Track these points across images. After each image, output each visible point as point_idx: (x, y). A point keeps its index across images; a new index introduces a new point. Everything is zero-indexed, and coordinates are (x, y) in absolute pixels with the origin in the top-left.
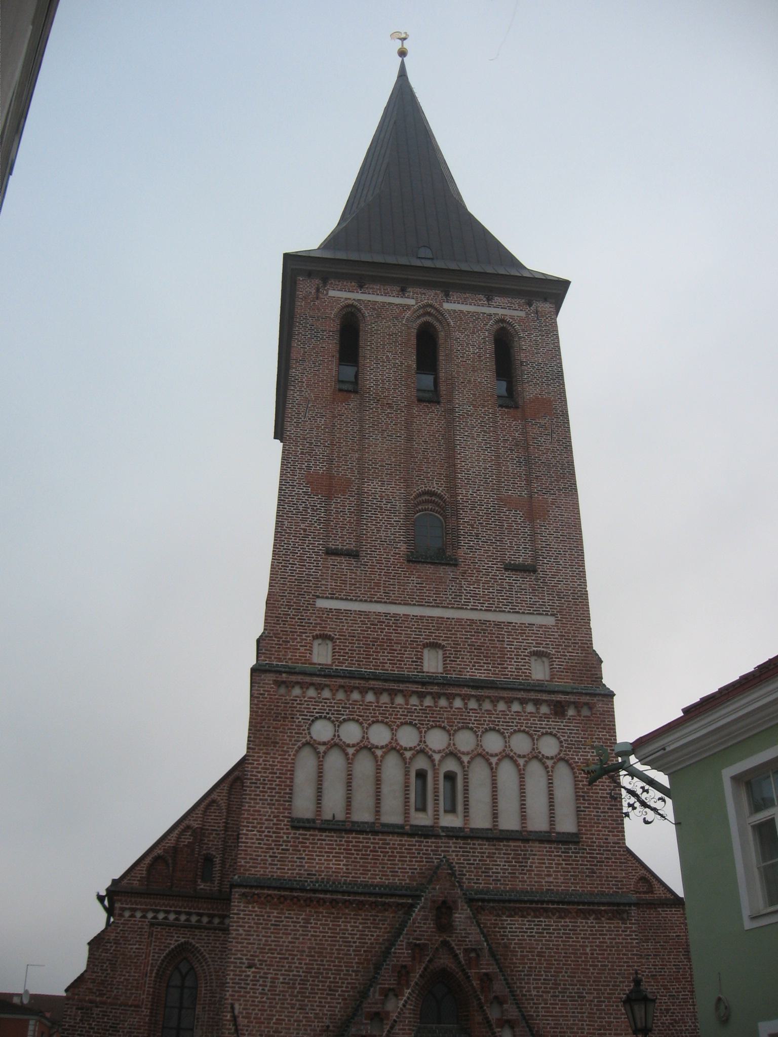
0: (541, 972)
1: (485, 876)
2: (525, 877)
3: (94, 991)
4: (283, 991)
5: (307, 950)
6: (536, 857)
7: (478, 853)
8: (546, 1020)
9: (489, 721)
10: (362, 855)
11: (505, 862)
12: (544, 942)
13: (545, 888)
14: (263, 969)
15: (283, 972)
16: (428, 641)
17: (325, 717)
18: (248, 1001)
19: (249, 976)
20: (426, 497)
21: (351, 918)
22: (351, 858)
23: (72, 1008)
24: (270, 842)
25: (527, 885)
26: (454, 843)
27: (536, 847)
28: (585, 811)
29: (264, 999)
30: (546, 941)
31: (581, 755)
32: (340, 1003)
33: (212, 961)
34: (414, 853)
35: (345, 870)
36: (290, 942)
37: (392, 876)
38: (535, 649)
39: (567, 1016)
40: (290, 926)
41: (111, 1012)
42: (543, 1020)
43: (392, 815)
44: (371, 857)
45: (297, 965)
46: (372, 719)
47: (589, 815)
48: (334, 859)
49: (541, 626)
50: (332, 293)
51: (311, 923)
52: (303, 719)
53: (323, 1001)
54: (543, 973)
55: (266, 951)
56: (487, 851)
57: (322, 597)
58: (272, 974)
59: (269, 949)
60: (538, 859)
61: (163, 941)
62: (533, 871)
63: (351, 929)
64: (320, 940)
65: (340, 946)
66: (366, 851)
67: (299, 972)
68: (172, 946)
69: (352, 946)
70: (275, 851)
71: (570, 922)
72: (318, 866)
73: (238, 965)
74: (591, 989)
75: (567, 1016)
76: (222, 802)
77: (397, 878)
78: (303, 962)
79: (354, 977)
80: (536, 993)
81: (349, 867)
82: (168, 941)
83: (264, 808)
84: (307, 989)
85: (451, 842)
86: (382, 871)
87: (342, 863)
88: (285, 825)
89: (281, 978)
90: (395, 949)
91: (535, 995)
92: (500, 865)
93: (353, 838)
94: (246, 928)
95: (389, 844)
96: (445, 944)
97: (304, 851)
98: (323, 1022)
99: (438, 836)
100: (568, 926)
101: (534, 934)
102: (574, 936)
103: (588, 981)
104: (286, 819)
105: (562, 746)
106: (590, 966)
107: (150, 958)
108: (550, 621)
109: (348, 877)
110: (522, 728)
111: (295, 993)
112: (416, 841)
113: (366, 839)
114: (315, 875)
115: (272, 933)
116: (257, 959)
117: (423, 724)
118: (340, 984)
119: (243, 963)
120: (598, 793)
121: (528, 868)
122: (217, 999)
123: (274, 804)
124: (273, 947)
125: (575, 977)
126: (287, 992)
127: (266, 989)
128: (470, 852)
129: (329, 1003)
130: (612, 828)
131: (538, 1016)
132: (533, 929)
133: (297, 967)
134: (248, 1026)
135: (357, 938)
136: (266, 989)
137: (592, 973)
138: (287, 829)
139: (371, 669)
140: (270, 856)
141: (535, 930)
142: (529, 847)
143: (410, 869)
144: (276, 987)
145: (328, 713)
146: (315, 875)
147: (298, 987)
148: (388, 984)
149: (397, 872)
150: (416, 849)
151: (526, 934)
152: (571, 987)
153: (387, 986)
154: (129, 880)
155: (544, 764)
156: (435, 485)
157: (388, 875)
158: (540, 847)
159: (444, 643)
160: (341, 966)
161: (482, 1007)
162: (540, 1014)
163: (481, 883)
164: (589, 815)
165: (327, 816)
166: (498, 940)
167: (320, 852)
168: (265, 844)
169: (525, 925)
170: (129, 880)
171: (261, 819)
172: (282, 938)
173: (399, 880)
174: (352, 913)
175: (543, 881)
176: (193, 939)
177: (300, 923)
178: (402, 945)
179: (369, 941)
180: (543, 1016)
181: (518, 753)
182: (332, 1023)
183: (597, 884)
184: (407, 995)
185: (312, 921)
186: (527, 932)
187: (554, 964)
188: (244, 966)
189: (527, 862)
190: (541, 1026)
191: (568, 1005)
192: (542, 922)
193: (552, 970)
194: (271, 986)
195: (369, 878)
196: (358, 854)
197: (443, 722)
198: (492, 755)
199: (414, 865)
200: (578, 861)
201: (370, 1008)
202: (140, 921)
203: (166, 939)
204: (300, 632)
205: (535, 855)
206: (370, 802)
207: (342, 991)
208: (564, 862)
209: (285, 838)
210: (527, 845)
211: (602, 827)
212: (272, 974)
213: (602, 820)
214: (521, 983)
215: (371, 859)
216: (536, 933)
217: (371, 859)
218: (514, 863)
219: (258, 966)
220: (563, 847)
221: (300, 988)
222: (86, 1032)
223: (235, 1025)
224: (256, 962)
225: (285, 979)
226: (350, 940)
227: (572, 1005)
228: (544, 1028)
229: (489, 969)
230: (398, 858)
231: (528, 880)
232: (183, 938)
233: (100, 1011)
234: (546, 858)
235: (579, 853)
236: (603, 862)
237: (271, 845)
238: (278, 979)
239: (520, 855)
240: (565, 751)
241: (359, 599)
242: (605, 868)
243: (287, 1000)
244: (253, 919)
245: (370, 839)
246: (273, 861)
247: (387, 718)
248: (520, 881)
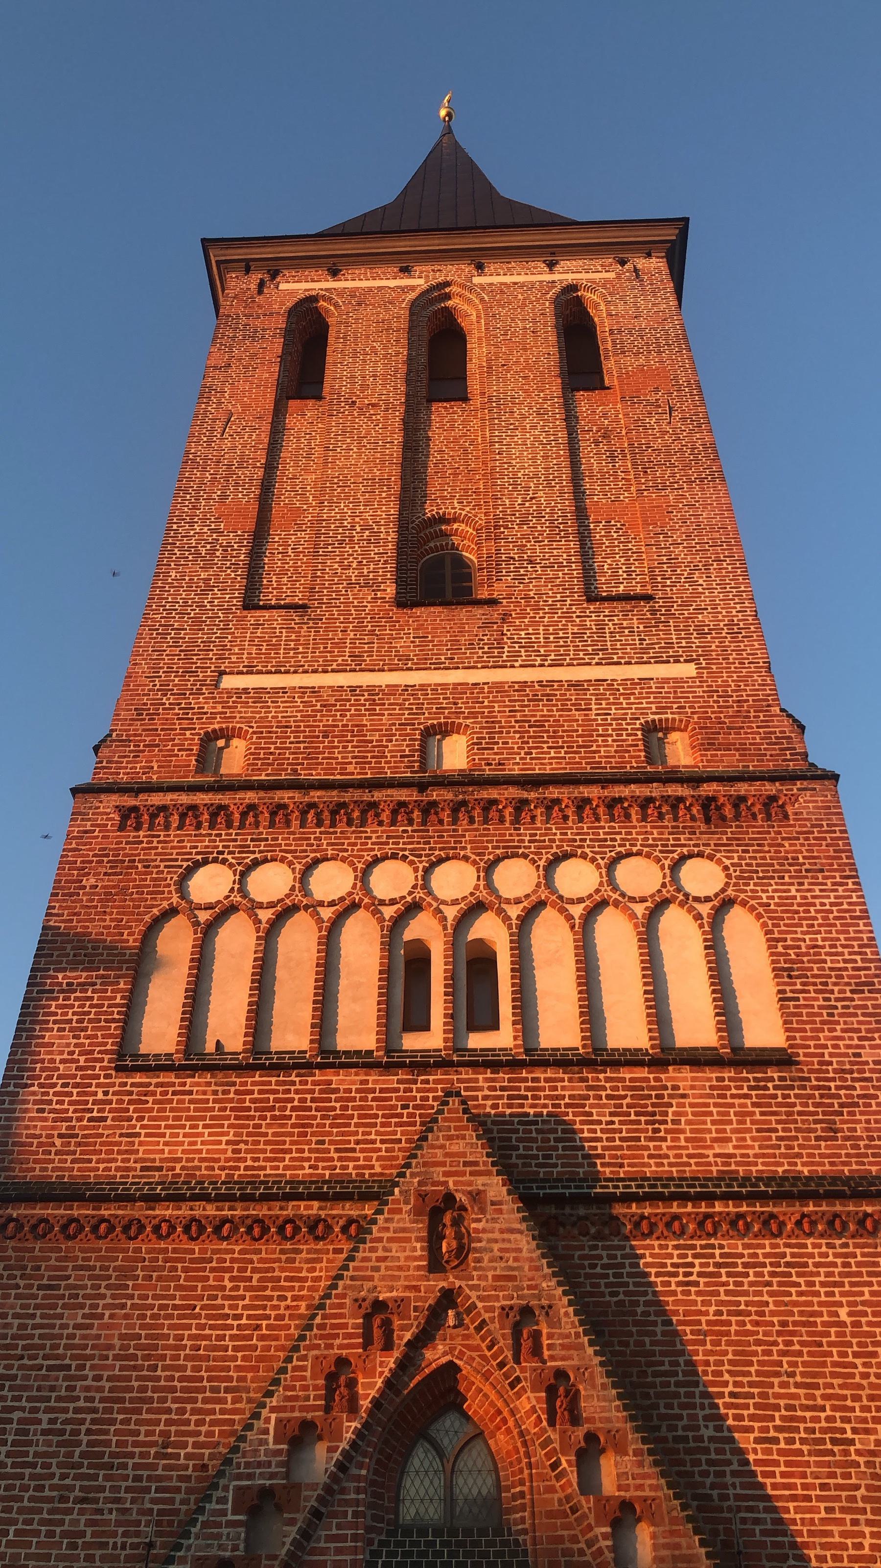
0: (720, 1374)
1: (564, 1148)
2: (664, 1145)
5: (117, 1342)
6: (687, 1101)
7: (546, 1097)
8: (750, 1509)
9: (561, 840)
10: (273, 1118)
11: (611, 1114)
12: (723, 1297)
13: (714, 1169)
15: (52, 1404)
16: (435, 722)
17: (215, 860)
21: (233, 1260)
22: (248, 1126)
24: (66, 1106)
25: (671, 1165)
26: (486, 1080)
27: (685, 1079)
28: (798, 999)
30: (727, 1293)
31: (775, 891)
32: (188, 1479)
34: (394, 1107)
35: (229, 1154)
36: (77, 1327)
37: (340, 1159)
38: (656, 717)
39: (808, 1498)
40: (84, 1287)
42: (739, 1509)
45: (89, 1382)
46: (312, 855)
47: (806, 1006)
48: (207, 1131)
49: (666, 680)
50: (283, 286)
51: (136, 1278)
52: (166, 867)
53: (145, 1473)
54: (727, 1377)
55: (19, 1352)
56: (567, 1093)
57: (231, 673)
58: (23, 1409)
59: (24, 1348)
60: (692, 1105)
62: (683, 1131)
63: (229, 1285)
64: (153, 1317)
66: (284, 1109)
67: (91, 1400)
69: (231, 1327)
71: (787, 1245)
72: (167, 1149)
74: (865, 1420)
75: (808, 1498)
77: (351, 1164)
78: (106, 1374)
79: (229, 1406)
80: (710, 1432)
81: (242, 1146)
83: (61, 1037)
85: (481, 1077)
86: (317, 1151)
87: (224, 1139)
89: (45, 1417)
90: (324, 1317)
91: (711, 1439)
92: (599, 1122)
93: (254, 1084)
98: (137, 1534)
100: (784, 1255)
101: (694, 1278)
102: (801, 1280)
103: (856, 1398)
105: (729, 876)
106: (856, 1355)
108: (688, 670)
109: (238, 1168)
110: (635, 849)
111: (76, 1458)
112: (399, 1082)
113: (284, 1083)
114: (160, 1169)
117: (420, 856)
118: (192, 1427)
120: (825, 961)
121: (670, 1126)
123: (85, 1029)
124: (36, 1341)
125: (816, 1386)
126: (55, 1455)
128: (526, 1098)
129: (159, 1479)
130: (868, 1031)
131: (725, 1497)
132: (692, 1265)
133: (87, 1389)
135: (245, 1307)
137: (865, 1376)
138: (107, 1076)
139: (319, 774)
141: (697, 1269)
142: (669, 1079)
143: (383, 1142)
144: (29, 1443)
145: (222, 853)
146: (160, 1169)
147: (85, 1439)
148: (302, 1409)
149: (353, 1150)
150: (398, 1099)
151: (673, 1280)
152: (808, 1414)
153: (297, 1414)
155: (691, 910)
156: (456, 505)
157: (332, 1160)
158: (694, 1079)
160: (201, 1379)
162: (731, 1492)
163: (555, 1165)
164: (806, 1006)
166: (602, 1295)
167: (176, 1118)
169: (671, 1256)
172: (61, 1316)
173: (356, 1167)
174: (237, 1248)
175: (710, 1152)
177: (109, 1277)
178: (341, 1306)
179: (273, 1313)
180: (738, 1497)
183: (848, 1155)
184: (349, 1435)
185: (139, 1272)
186: (675, 1275)
187: (755, 1353)
189: (666, 1114)
190: (737, 1526)
191: (807, 1464)
192: (713, 1247)
193: (752, 1369)
194: (14, 1443)
195: (286, 1168)
197: (464, 848)
198: (571, 901)
199: (395, 1133)
200: (794, 1105)
201: (250, 1477)
204: (181, 729)
205: (684, 1096)
206: (305, 1014)
208: (757, 1110)
209: (100, 1096)
210: (663, 1076)
211: (843, 1030)
212: (23, 1409)
213: (841, 1015)
214: (669, 1406)
215: (293, 1126)
216: (700, 1274)
217: (293, 1126)
218: (633, 1117)
220: (750, 1076)
221: (90, 1444)
226: (227, 1311)
227: (818, 1464)
228: (744, 1532)
229: (570, 1358)
230: (356, 1120)
231: (671, 1153)
234: (711, 1101)
235: (792, 1088)
236: (857, 1105)
237: (67, 1111)
239: (649, 1097)
240: (735, 885)
241: (301, 669)
242: (863, 1118)
243: (53, 1475)
245: (293, 1083)
247: (347, 850)
248: (650, 1156)
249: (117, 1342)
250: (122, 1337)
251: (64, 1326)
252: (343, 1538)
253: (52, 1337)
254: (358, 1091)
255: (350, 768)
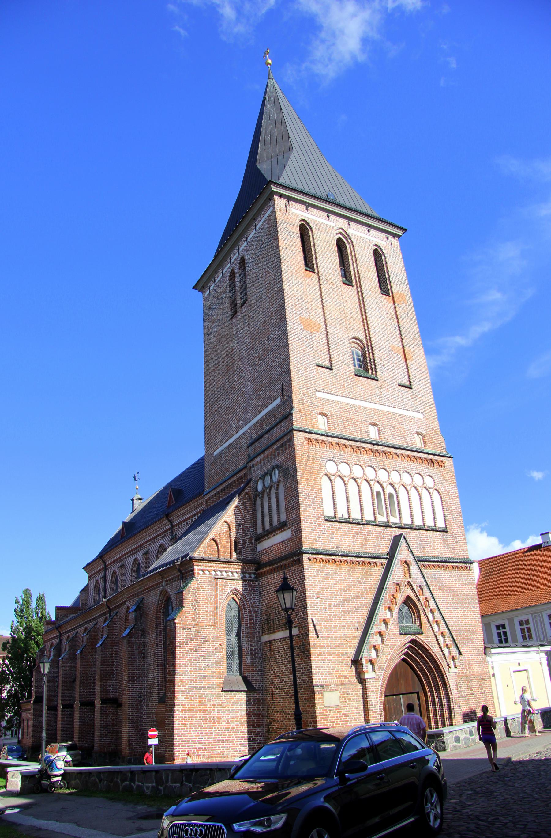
3: (190, 618)
4: (335, 611)
5: (343, 588)
14: (324, 599)
18: (319, 616)
19: (318, 603)
20: (359, 342)
23: (180, 629)
29: (327, 615)
33: (249, 599)
41: (201, 630)
43: (369, 516)
44: (363, 538)
53: (353, 615)
61: (224, 588)
65: (358, 585)
67: (341, 600)
68: (229, 591)
70: (320, 534)
73: (312, 597)
76: (241, 507)
82: (226, 588)
84: (345, 609)
88: (322, 520)
89: (333, 603)
94: (313, 577)
95: (370, 531)
96: (409, 582)
97: (333, 534)
99: (391, 527)
104: (322, 516)
107: (218, 598)
112: (382, 530)
114: (340, 547)
115: (339, 580)
116: (320, 593)
119: (314, 596)
122: (254, 620)
127: (327, 609)
134: (321, 630)
136: (327, 609)
140: (318, 537)
144: (331, 608)
154: (199, 553)
159: (378, 423)
161: (426, 614)
165: (339, 515)
168: (314, 530)
170: (199, 553)
171: (310, 516)
176: (238, 586)
181: (418, 485)
182: (359, 626)
188: (314, 597)
196: (357, 536)
201: (381, 617)
202: (209, 577)
203: (225, 587)
207: (361, 609)
219: (321, 597)
221: (342, 609)
222: (190, 642)
223: (315, 629)
224: (320, 595)
225: (334, 604)
232: (233, 586)
233: (195, 630)
238: (332, 604)
244: (316, 572)
246: (319, 539)
249: (343, 588)
250: (343, 587)
251: (332, 584)
252: (395, 627)
253: (330, 586)
254: (375, 531)
255: (355, 434)
